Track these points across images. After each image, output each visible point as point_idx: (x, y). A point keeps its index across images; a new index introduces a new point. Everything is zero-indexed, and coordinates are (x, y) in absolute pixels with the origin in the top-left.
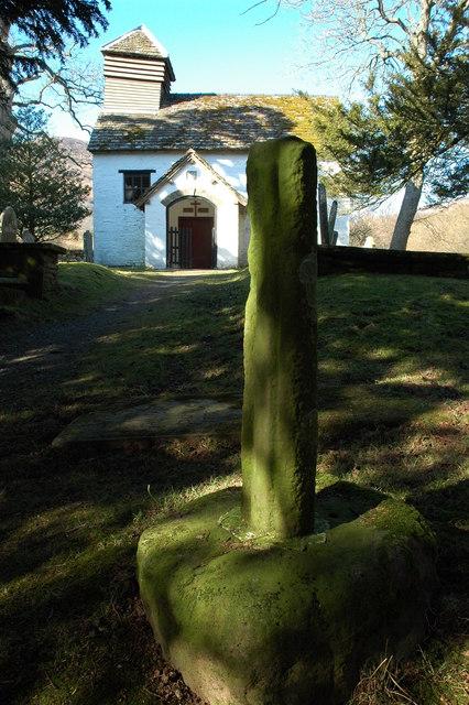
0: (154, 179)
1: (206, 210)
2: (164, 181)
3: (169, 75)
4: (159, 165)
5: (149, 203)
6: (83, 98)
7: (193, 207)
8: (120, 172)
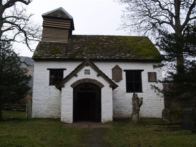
0: (66, 74)
2: (74, 74)
3: (72, 28)
4: (69, 68)
6: (32, 38)
8: (48, 69)
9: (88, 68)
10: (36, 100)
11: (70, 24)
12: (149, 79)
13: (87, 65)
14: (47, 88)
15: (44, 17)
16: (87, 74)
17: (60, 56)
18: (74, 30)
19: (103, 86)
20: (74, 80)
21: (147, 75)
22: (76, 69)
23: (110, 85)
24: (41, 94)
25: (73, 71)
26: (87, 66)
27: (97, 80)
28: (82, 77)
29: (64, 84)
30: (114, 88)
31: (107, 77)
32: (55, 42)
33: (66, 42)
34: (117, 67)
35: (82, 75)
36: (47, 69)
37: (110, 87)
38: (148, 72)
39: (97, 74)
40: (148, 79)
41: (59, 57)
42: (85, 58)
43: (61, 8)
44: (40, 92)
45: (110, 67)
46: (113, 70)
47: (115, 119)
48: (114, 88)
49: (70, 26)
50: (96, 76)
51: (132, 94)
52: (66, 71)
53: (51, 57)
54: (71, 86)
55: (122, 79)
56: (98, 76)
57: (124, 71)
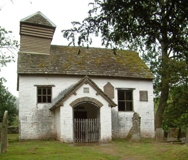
1: (83, 108)
2: (72, 91)
5: (63, 106)
8: (35, 86)
9: (87, 86)
12: (140, 98)
16: (87, 92)
17: (48, 71)
19: (102, 105)
26: (86, 84)
32: (36, 53)
33: (49, 54)
34: (109, 84)
35: (80, 94)
38: (140, 91)
40: (140, 98)
42: (76, 73)
43: (39, 12)
50: (96, 95)
54: (71, 105)
55: (114, 98)
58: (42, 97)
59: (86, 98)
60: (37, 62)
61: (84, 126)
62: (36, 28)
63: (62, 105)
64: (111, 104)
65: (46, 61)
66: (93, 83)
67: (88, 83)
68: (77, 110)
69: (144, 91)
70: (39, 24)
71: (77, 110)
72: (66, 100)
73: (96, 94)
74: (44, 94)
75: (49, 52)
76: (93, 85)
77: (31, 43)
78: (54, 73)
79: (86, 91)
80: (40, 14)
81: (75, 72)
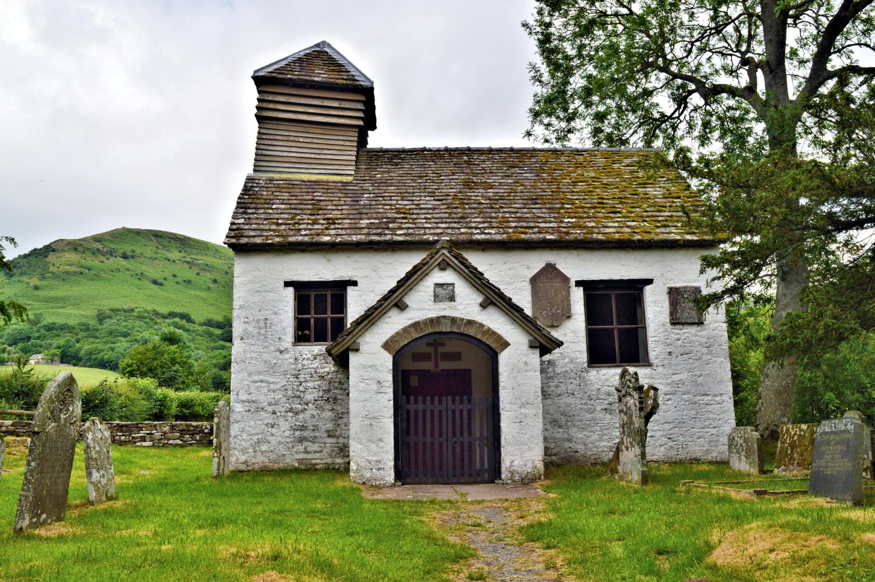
1: (455, 356)
3: (370, 122)
4: (370, 280)
7: (430, 350)
8: (287, 284)
9: (448, 277)
10: (244, 401)
11: (361, 106)
13: (444, 266)
14: (287, 356)
15: (260, 80)
16: (444, 300)
18: (373, 127)
19: (506, 344)
20: (393, 324)
21: (666, 298)
22: (401, 283)
23: (531, 338)
24: (261, 377)
25: (392, 292)
26: (443, 270)
27: (484, 323)
28: (424, 312)
29: (358, 341)
30: (544, 350)
31: (520, 310)
34: (550, 269)
35: (422, 305)
36: (283, 284)
37: (531, 347)
39: (480, 299)
41: (329, 235)
44: (259, 373)
45: (526, 271)
46: (534, 280)
47: (547, 465)
48: (544, 350)
49: (361, 115)
50: (479, 308)
51: (619, 371)
52: (355, 288)
53: (300, 238)
54: (386, 346)
55: (569, 317)
56: (483, 306)
57: (579, 283)
58: (312, 321)
59: (443, 321)
60: (299, 206)
61: (436, 424)
62: (311, 93)
63: (354, 347)
64: (538, 338)
65: (334, 203)
66: (469, 266)
67: (448, 264)
68: (437, 366)
69: (686, 287)
70: (314, 81)
71: (437, 366)
72: (366, 329)
73: (481, 305)
74: (320, 313)
75: (353, 172)
76: (467, 271)
77: (290, 144)
78: (354, 238)
79: (444, 293)
80: (326, 49)
81: (427, 231)
